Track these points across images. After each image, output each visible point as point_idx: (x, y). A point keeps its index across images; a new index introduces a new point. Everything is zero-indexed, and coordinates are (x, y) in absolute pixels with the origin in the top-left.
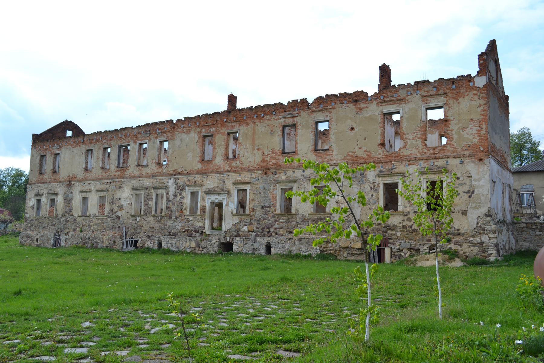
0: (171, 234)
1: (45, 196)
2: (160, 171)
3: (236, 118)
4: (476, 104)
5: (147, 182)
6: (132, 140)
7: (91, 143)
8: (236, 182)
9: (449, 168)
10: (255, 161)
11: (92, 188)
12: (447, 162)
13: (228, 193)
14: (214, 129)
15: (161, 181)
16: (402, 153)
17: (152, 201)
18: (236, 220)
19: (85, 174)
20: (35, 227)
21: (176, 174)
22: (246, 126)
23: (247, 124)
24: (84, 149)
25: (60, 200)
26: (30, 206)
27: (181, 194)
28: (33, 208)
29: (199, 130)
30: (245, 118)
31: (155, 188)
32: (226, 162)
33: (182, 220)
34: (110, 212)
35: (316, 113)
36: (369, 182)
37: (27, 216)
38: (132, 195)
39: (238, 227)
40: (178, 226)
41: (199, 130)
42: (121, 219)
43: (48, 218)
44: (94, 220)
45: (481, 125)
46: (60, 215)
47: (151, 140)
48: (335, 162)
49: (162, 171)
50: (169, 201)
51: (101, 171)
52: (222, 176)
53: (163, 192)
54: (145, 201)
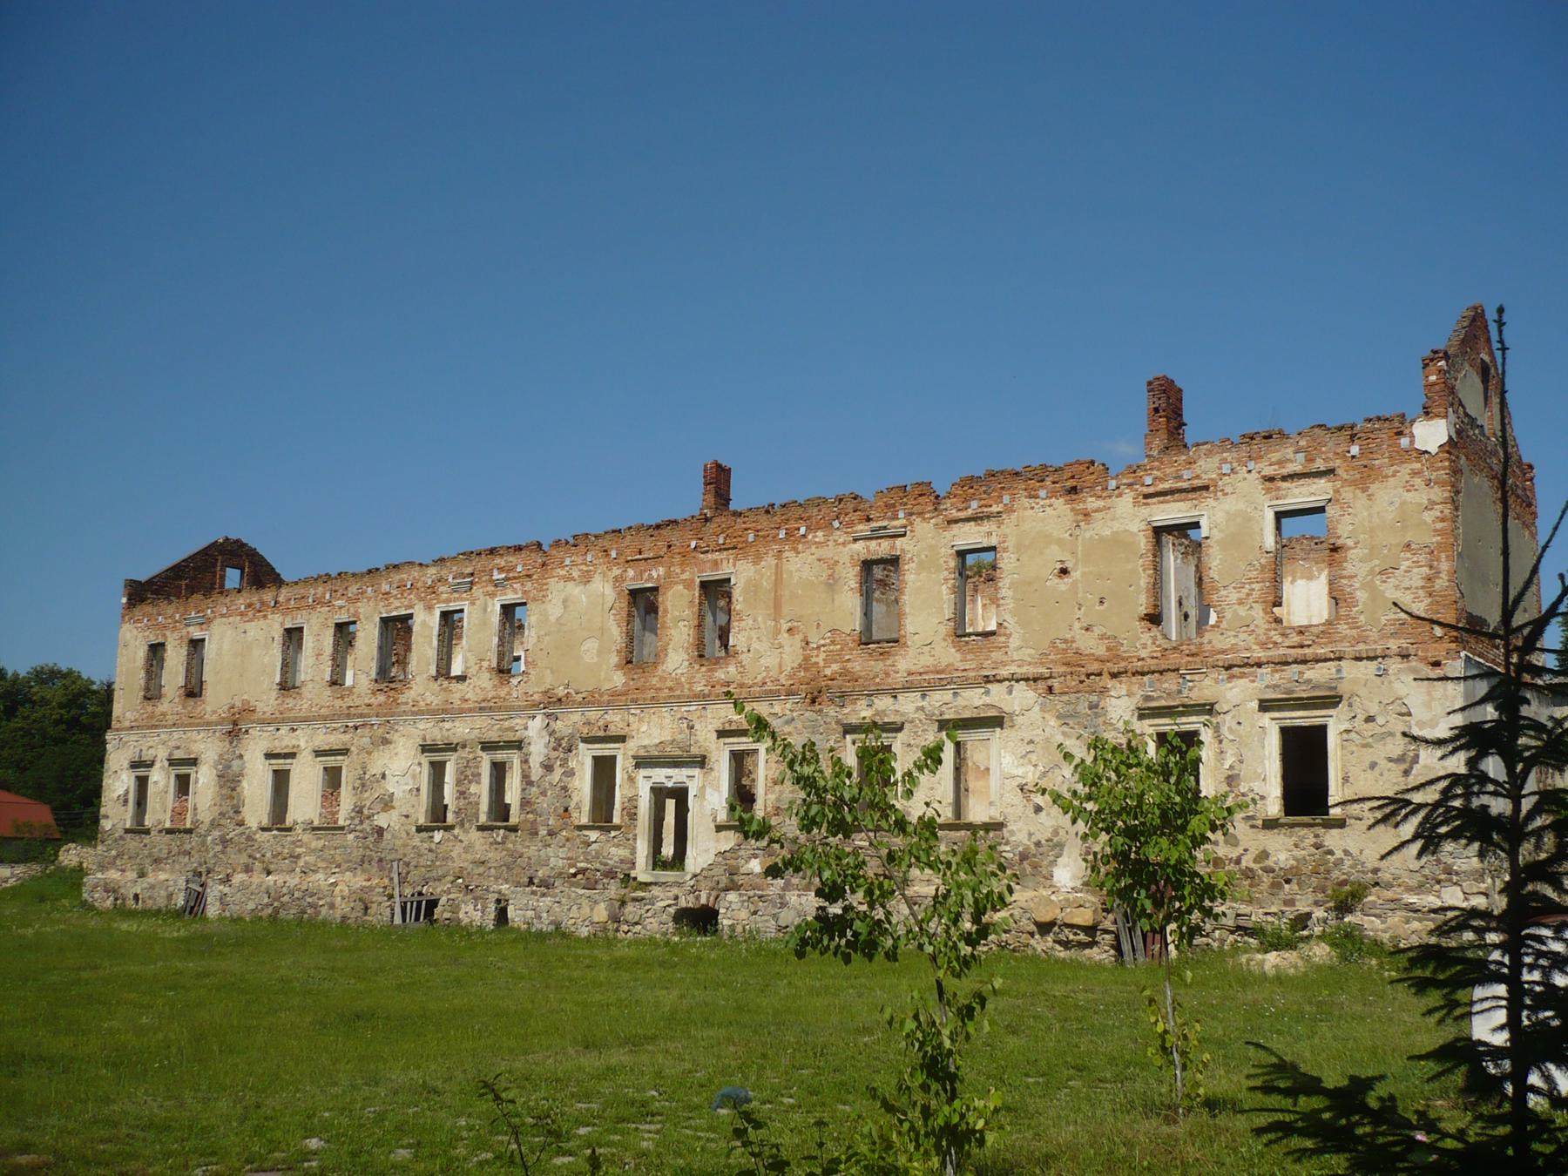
0: (536, 881)
1: (162, 767)
2: (502, 694)
3: (725, 539)
4: (1418, 500)
5: (461, 729)
6: (421, 599)
7: (298, 608)
8: (727, 727)
9: (1343, 688)
10: (780, 667)
11: (303, 745)
12: (1339, 671)
13: (701, 762)
14: (661, 570)
15: (507, 724)
16: (1210, 642)
17: (478, 783)
18: (729, 840)
19: (279, 701)
20: (130, 858)
21: (552, 703)
22: (755, 563)
23: (758, 559)
25: (204, 780)
27: (564, 762)
28: (126, 802)
29: (616, 571)
30: (751, 538)
31: (488, 746)
32: (697, 667)
33: (568, 840)
34: (353, 814)
35: (960, 525)
36: (1115, 729)
38: (420, 764)
39: (732, 862)
40: (557, 858)
41: (616, 571)
42: (387, 835)
43: (169, 831)
45: (1435, 563)
46: (207, 821)
47: (478, 603)
48: (1013, 669)
49: (509, 693)
50: (531, 783)
51: (328, 692)
52: (684, 709)
53: (514, 758)
54: (459, 783)
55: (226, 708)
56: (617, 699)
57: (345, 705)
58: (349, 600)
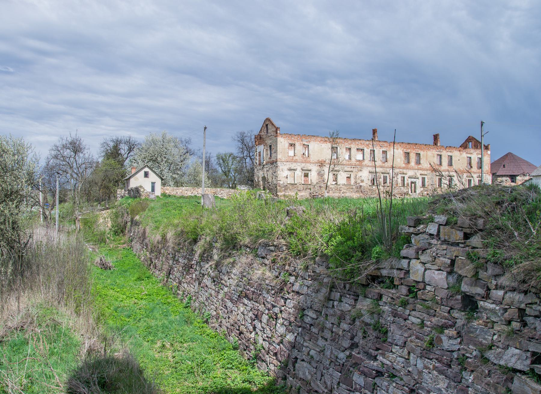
18: (422, 189)
23: (424, 151)
26: (284, 176)
29: (403, 149)
37: (281, 182)
41: (403, 149)
44: (343, 187)
56: (404, 168)
58: (349, 144)
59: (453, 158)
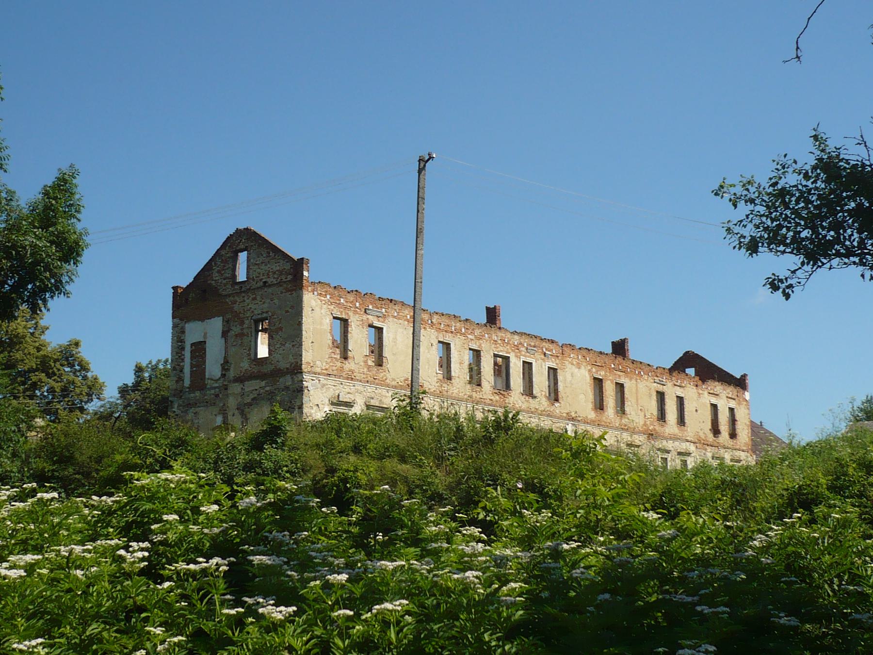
19: (438, 384)
24: (433, 337)
29: (589, 368)
55: (403, 379)
57: (478, 397)
59: (686, 402)
